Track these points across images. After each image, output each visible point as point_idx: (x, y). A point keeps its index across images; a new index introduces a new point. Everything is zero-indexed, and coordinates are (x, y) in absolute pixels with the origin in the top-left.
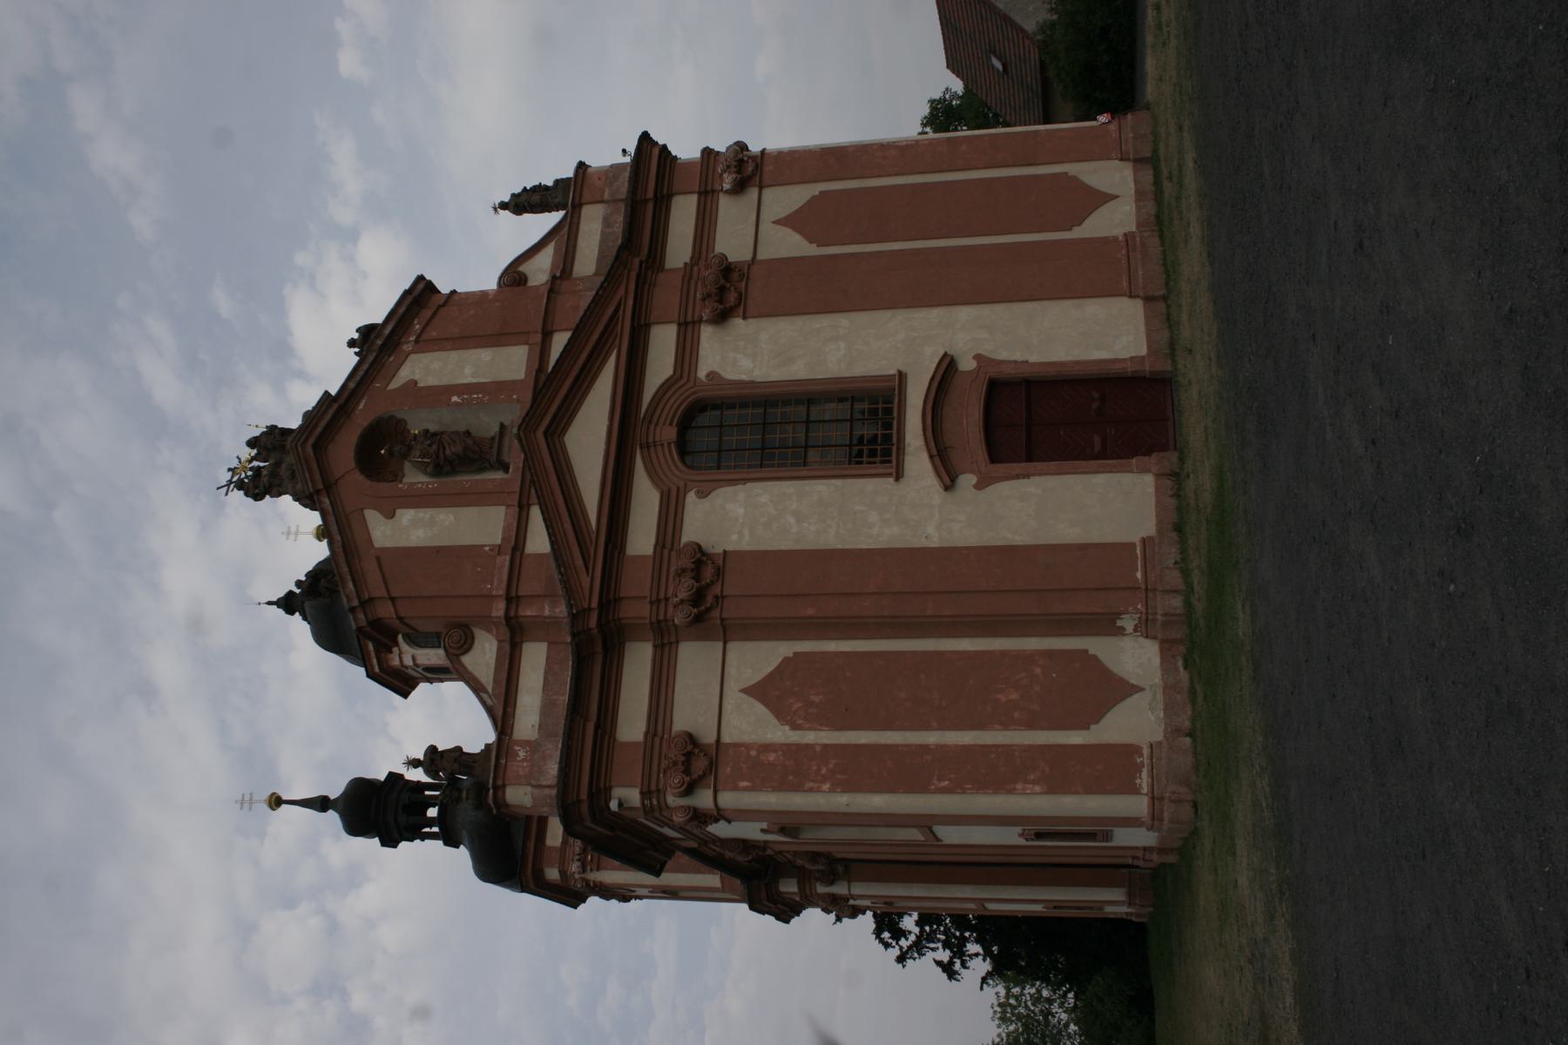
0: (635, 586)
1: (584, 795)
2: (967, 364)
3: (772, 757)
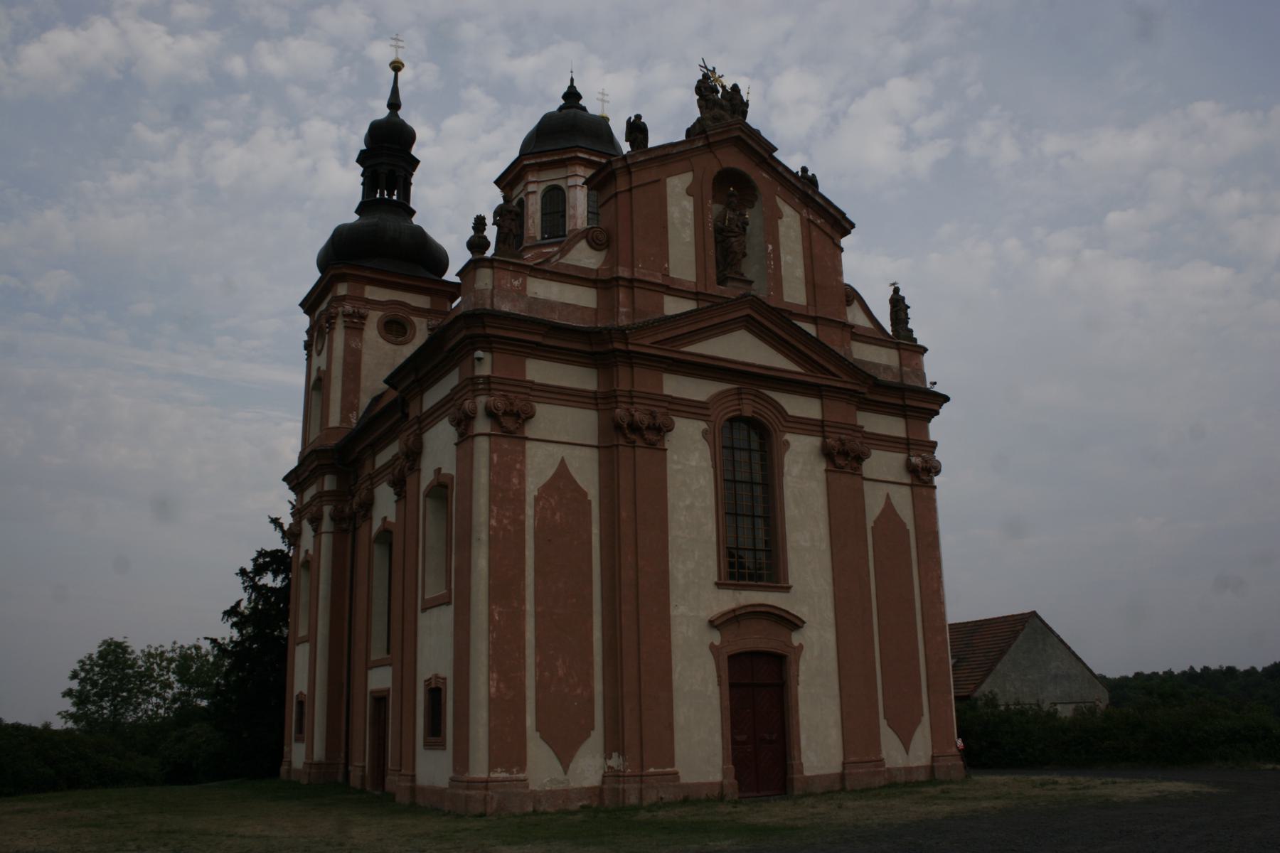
0: (643, 380)
1: (489, 331)
2: (796, 639)
3: (515, 481)
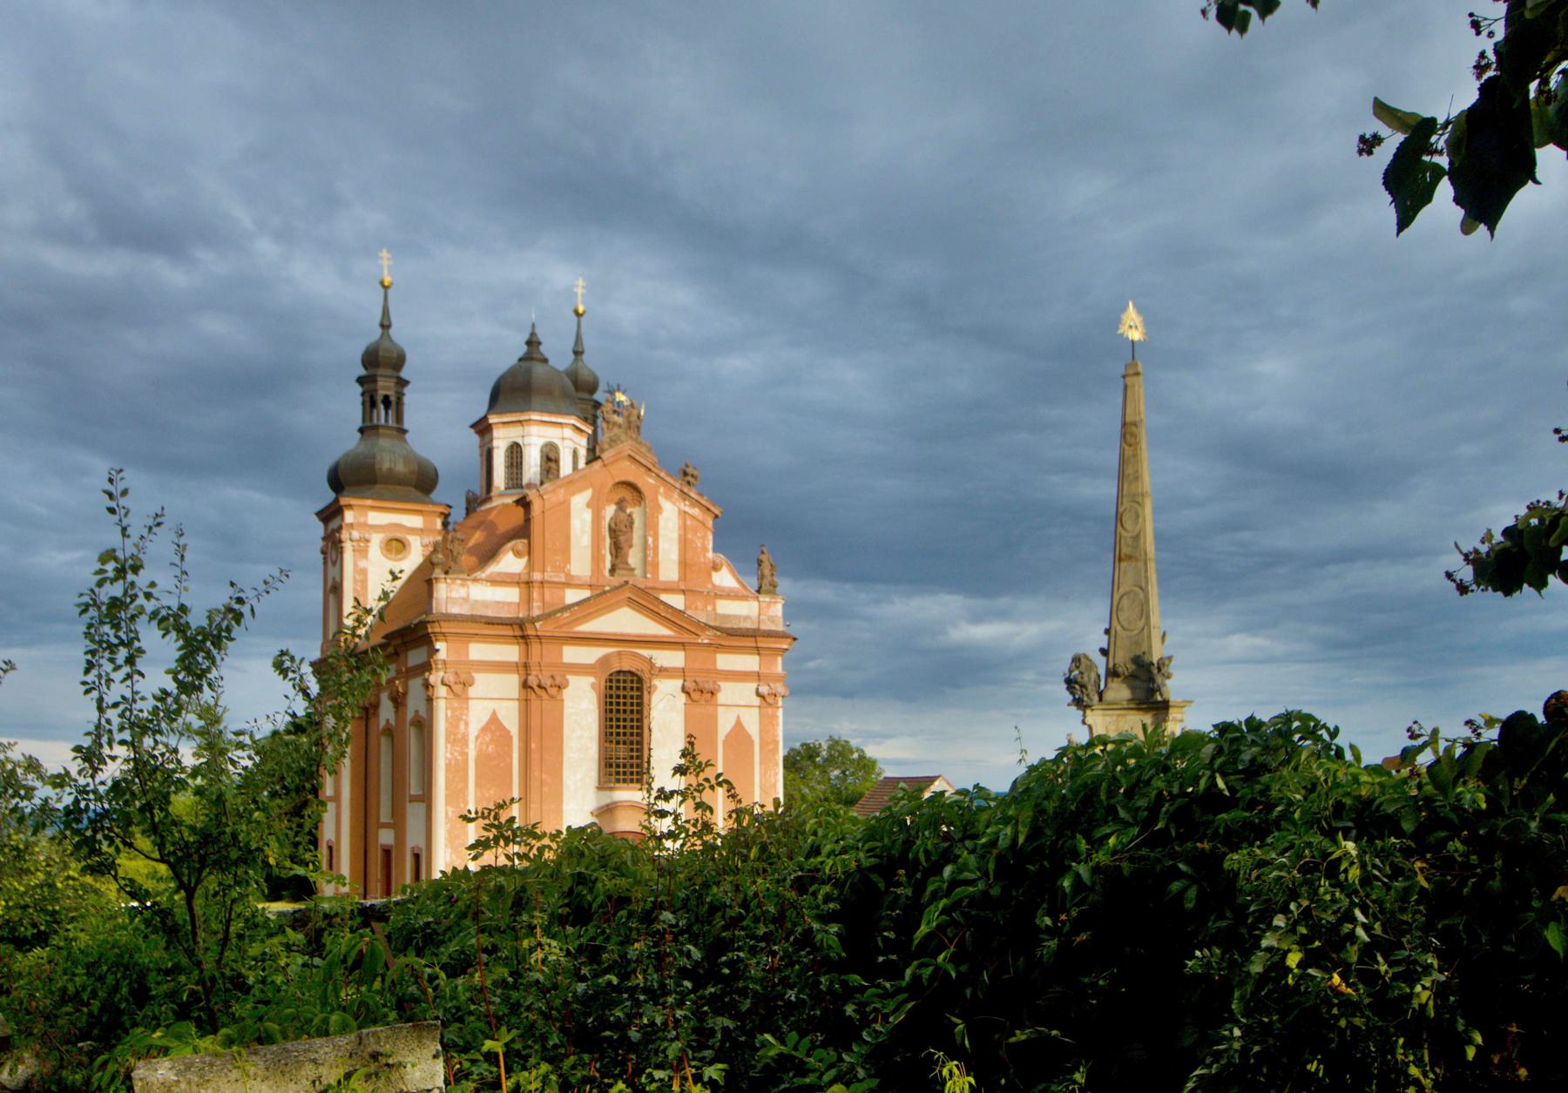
3: (462, 726)
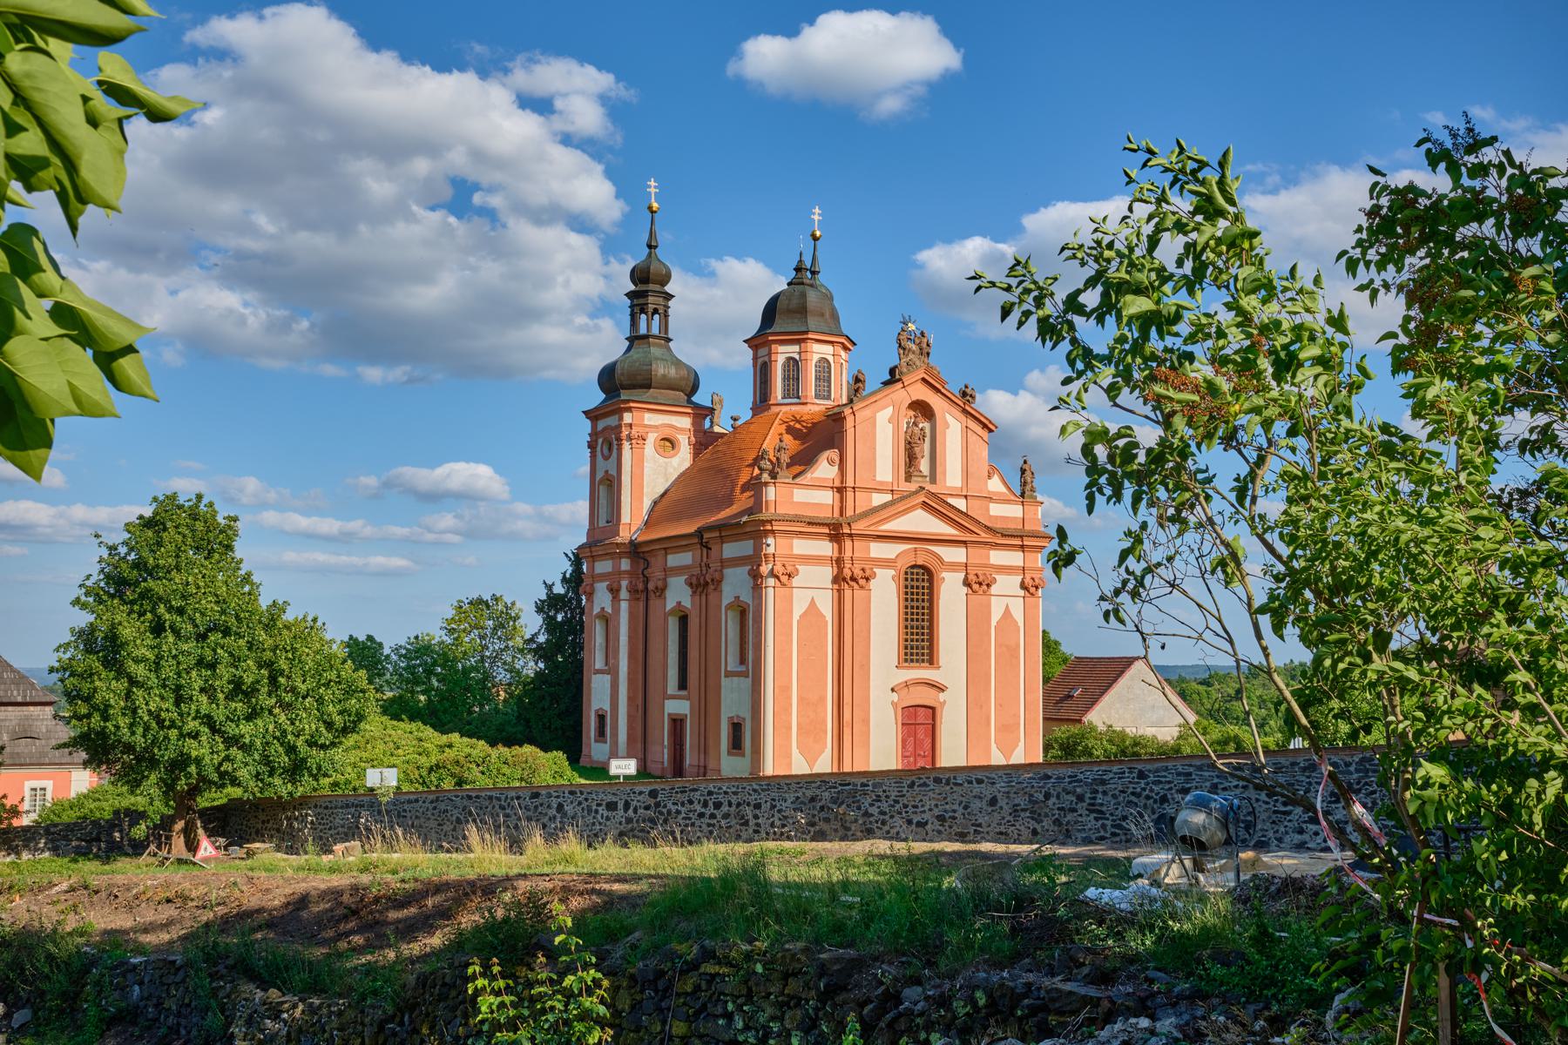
2: (942, 696)
